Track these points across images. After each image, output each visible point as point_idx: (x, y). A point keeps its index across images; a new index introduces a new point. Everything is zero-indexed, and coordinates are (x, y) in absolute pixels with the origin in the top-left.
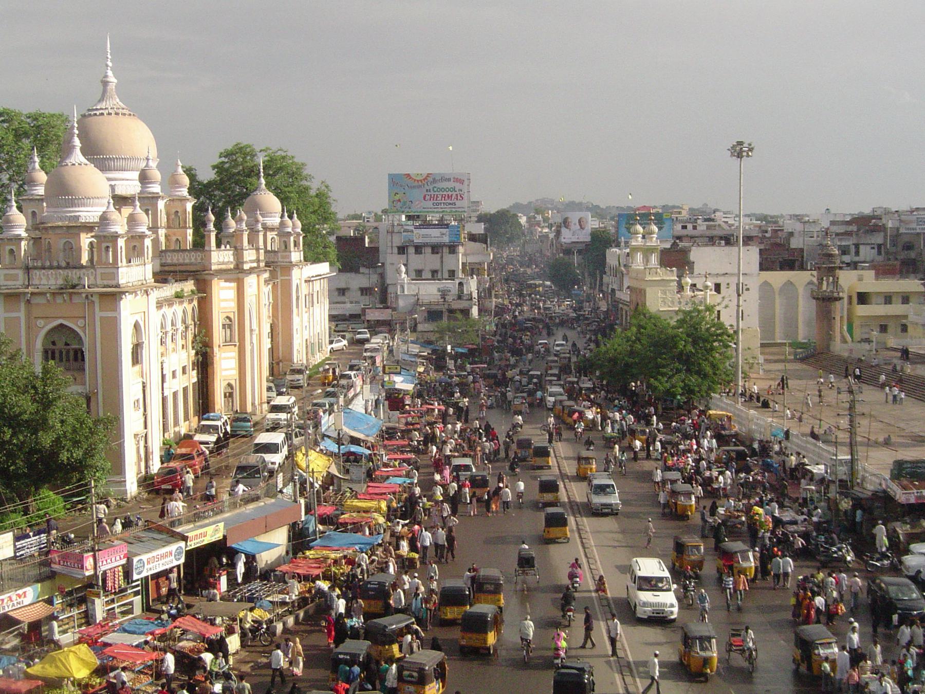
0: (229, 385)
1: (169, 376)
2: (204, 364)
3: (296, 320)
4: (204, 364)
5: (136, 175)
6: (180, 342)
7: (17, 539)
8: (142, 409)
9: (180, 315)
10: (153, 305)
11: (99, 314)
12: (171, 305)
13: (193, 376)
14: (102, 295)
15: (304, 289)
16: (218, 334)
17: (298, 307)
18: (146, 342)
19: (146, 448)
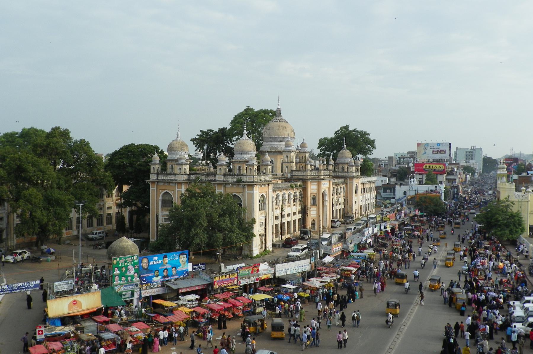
0: (313, 220)
1: (286, 216)
2: (304, 211)
3: (355, 198)
4: (304, 211)
5: (284, 143)
6: (292, 204)
7: (193, 265)
8: (264, 226)
9: (293, 194)
10: (271, 190)
11: (247, 192)
12: (287, 190)
13: (299, 216)
14: (248, 185)
15: (360, 187)
16: (309, 202)
17: (356, 192)
18: (267, 202)
19: (265, 240)
